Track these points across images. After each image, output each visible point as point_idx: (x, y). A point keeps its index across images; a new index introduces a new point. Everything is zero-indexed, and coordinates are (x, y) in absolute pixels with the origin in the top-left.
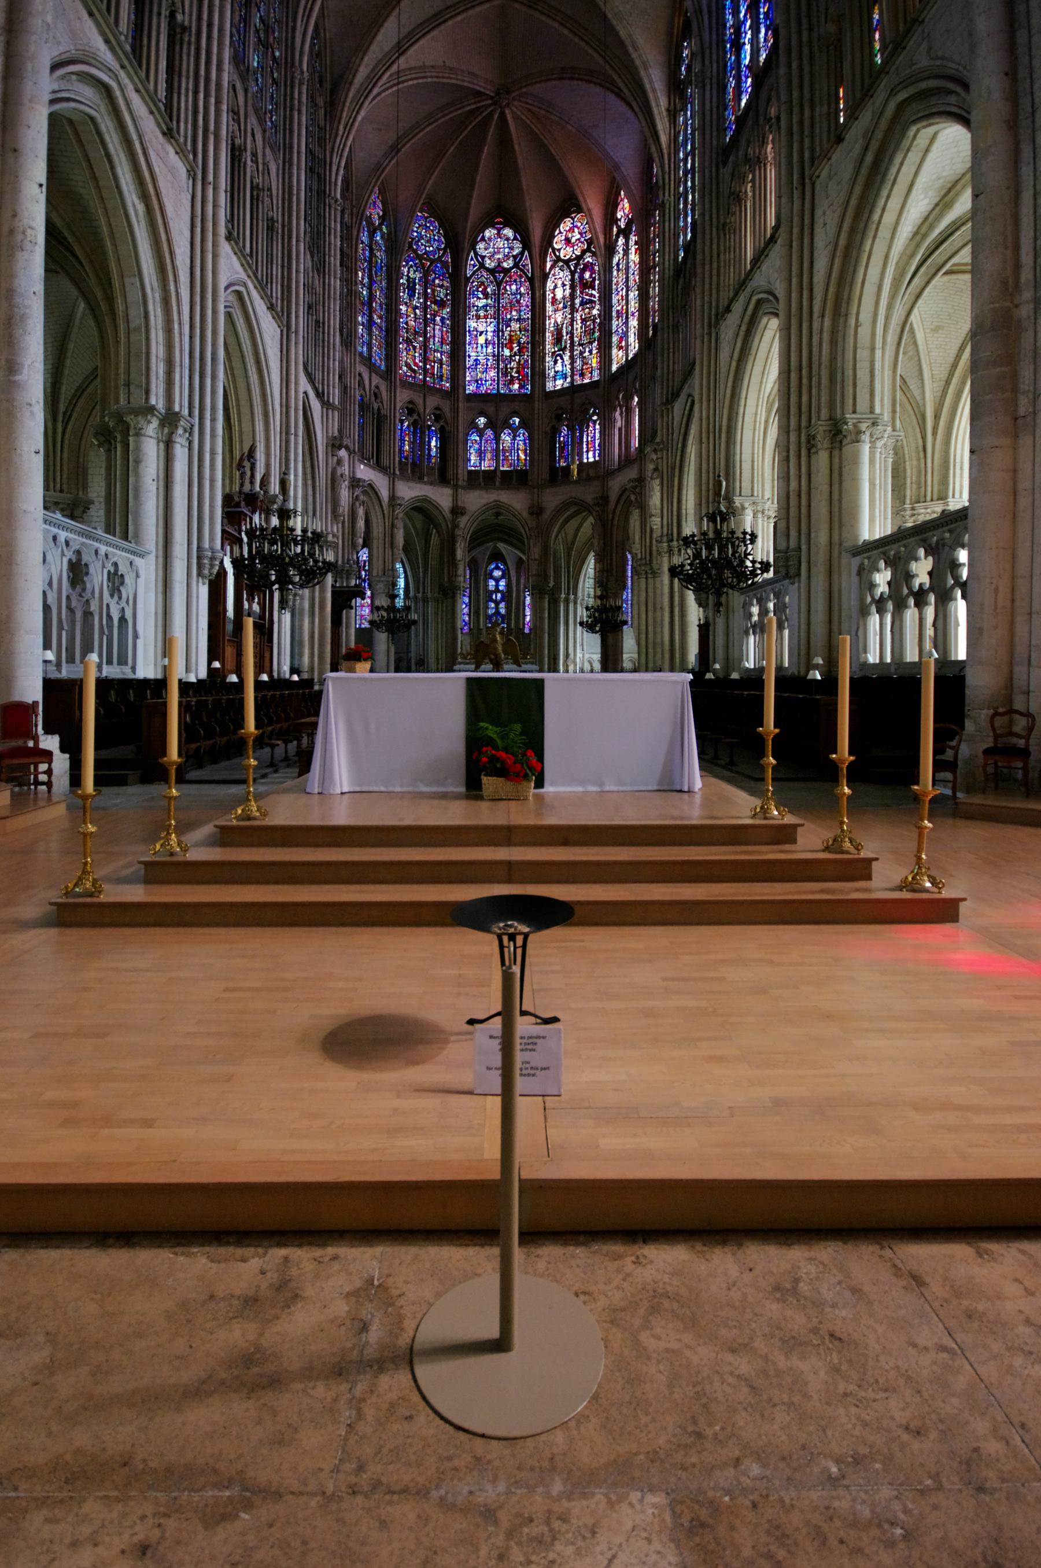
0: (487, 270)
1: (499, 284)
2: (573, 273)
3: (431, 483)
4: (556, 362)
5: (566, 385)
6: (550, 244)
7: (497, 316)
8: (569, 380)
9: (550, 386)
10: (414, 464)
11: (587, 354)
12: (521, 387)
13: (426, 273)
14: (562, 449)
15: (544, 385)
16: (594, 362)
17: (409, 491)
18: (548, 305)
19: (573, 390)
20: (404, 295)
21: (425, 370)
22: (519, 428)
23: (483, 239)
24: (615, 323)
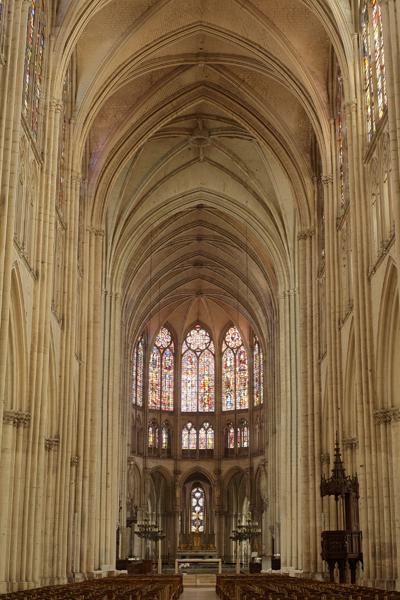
1: (198, 358)
2: (235, 355)
3: (163, 458)
6: (224, 338)
9: (224, 409)
12: (210, 408)
15: (221, 408)
16: (246, 399)
17: (152, 464)
18: (224, 369)
19: (236, 412)
20: (151, 368)
21: (161, 403)
24: (255, 383)
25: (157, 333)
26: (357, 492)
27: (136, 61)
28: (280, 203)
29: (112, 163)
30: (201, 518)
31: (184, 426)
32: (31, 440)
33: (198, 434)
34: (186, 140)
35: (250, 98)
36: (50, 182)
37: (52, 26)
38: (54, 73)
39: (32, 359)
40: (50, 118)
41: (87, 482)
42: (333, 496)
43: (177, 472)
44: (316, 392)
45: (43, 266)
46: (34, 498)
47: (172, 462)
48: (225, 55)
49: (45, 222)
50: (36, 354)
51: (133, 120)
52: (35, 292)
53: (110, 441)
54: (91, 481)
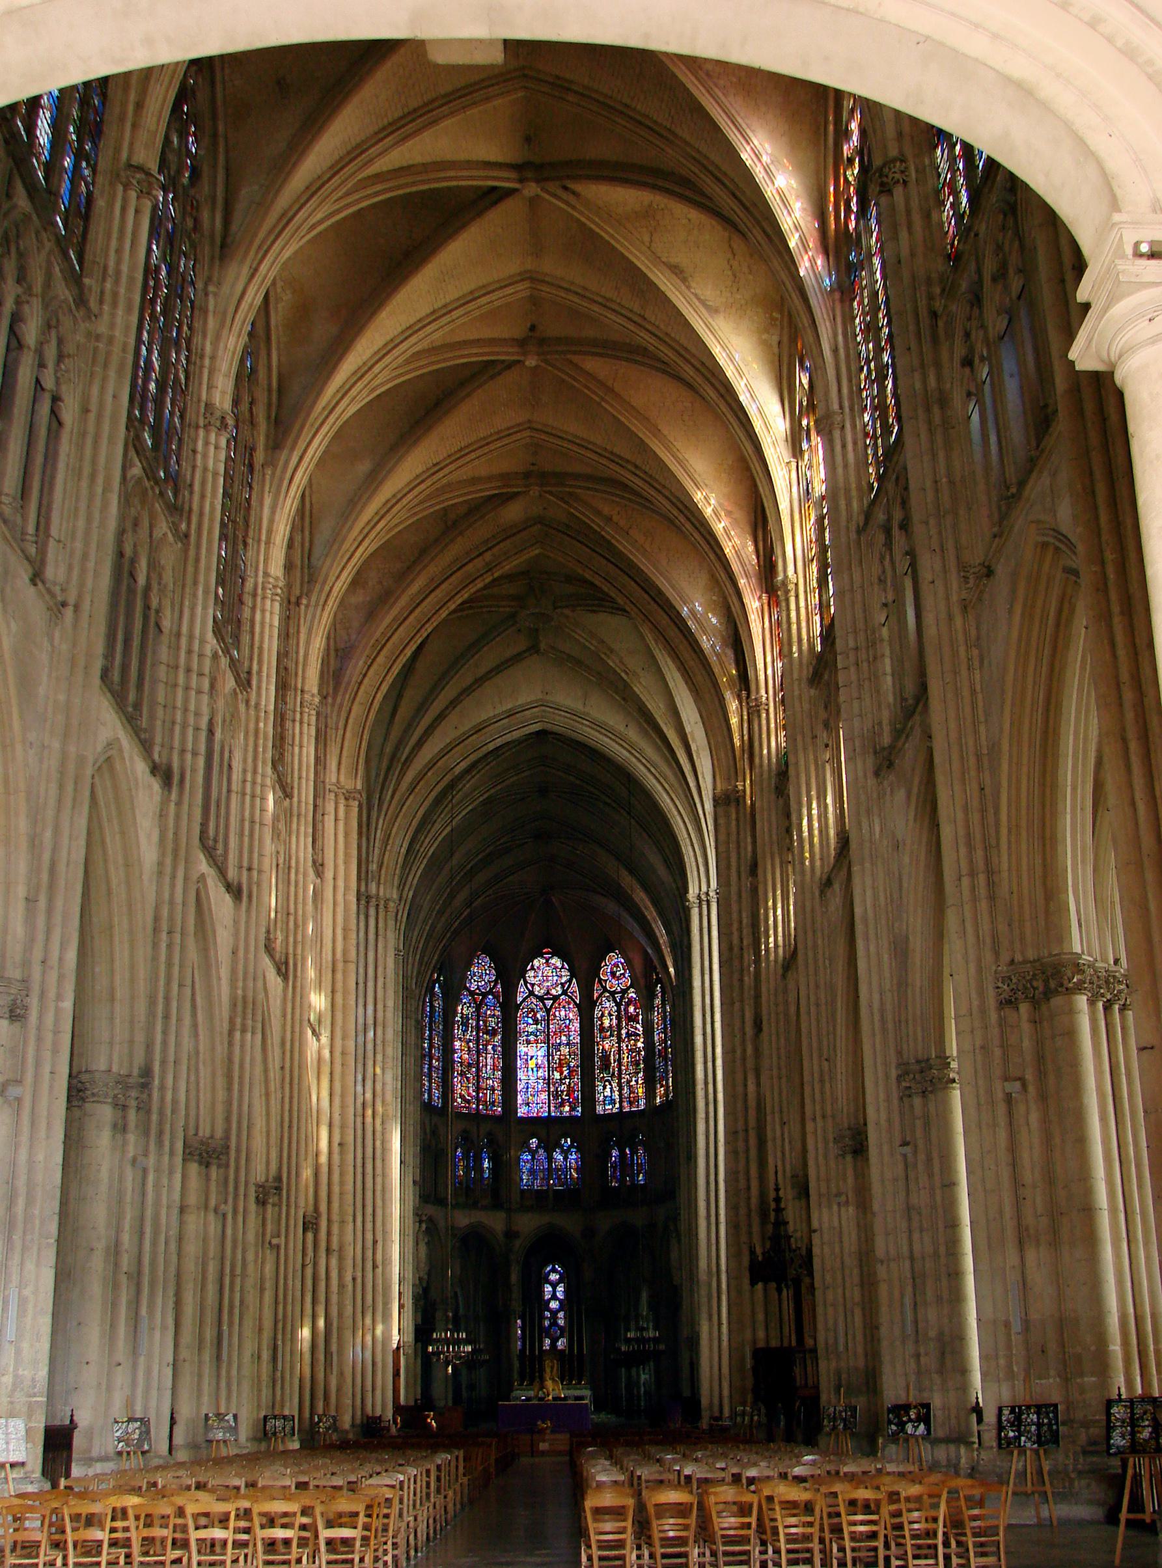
0: (537, 997)
1: (548, 1011)
2: (618, 1005)
3: (484, 1208)
4: (605, 1087)
5: (615, 1111)
7: (547, 1041)
8: (617, 1105)
9: (599, 1109)
10: (468, 1187)
11: (633, 1083)
12: (572, 1109)
13: (478, 1008)
14: (614, 1167)
17: (463, 1219)
21: (478, 1098)
22: (569, 1147)
23: (532, 968)
25: (469, 964)
26: (811, 1274)
27: (416, 492)
28: (688, 730)
29: (375, 666)
30: (561, 1322)
31: (525, 1146)
32: (231, 1189)
33: (550, 1159)
34: (513, 616)
35: (623, 545)
36: (261, 725)
37: (266, 449)
38: (270, 532)
39: (231, 1044)
40: (263, 611)
41: (334, 1262)
42: (773, 1285)
43: (510, 1234)
44: (751, 1087)
45: (250, 878)
46: (238, 1295)
47: (502, 1215)
48: (576, 476)
49: (253, 796)
50: (238, 1034)
51: (414, 588)
52: (236, 922)
53: (379, 1180)
54: (341, 1259)
